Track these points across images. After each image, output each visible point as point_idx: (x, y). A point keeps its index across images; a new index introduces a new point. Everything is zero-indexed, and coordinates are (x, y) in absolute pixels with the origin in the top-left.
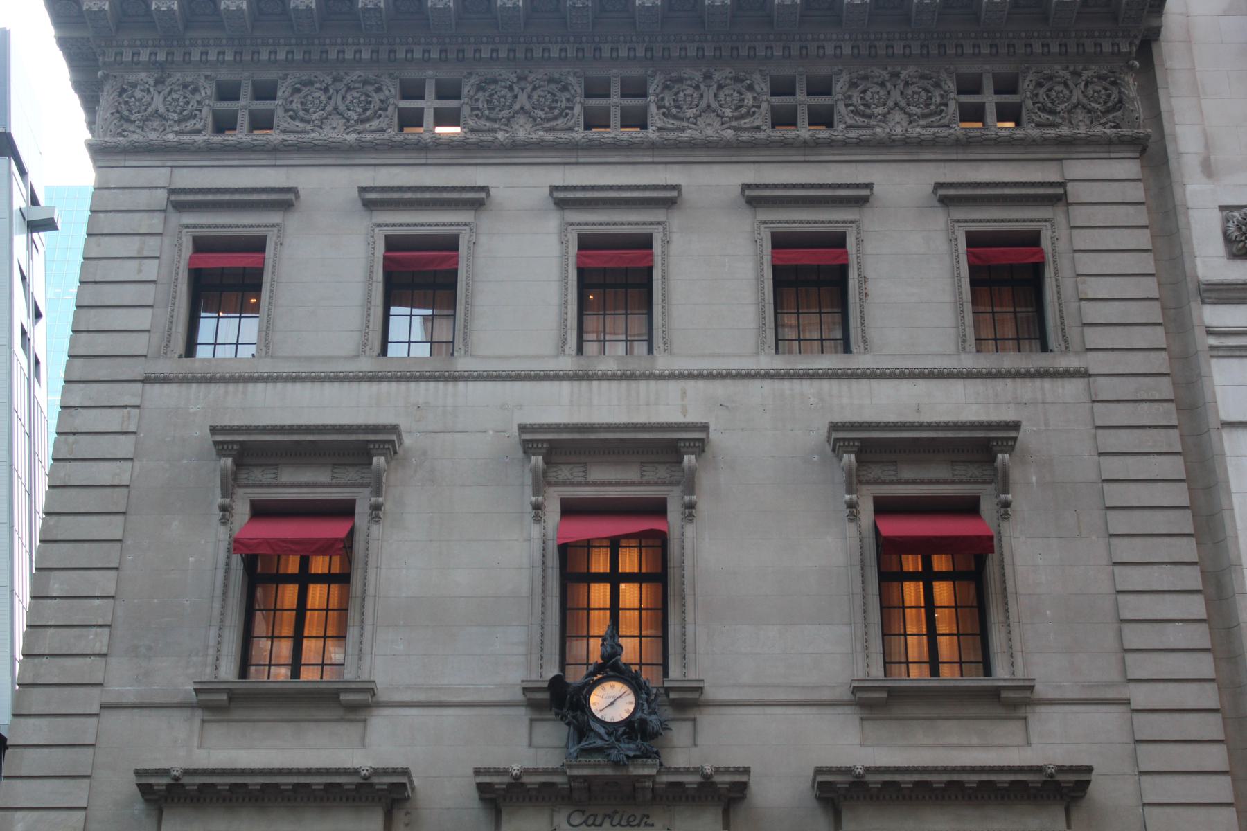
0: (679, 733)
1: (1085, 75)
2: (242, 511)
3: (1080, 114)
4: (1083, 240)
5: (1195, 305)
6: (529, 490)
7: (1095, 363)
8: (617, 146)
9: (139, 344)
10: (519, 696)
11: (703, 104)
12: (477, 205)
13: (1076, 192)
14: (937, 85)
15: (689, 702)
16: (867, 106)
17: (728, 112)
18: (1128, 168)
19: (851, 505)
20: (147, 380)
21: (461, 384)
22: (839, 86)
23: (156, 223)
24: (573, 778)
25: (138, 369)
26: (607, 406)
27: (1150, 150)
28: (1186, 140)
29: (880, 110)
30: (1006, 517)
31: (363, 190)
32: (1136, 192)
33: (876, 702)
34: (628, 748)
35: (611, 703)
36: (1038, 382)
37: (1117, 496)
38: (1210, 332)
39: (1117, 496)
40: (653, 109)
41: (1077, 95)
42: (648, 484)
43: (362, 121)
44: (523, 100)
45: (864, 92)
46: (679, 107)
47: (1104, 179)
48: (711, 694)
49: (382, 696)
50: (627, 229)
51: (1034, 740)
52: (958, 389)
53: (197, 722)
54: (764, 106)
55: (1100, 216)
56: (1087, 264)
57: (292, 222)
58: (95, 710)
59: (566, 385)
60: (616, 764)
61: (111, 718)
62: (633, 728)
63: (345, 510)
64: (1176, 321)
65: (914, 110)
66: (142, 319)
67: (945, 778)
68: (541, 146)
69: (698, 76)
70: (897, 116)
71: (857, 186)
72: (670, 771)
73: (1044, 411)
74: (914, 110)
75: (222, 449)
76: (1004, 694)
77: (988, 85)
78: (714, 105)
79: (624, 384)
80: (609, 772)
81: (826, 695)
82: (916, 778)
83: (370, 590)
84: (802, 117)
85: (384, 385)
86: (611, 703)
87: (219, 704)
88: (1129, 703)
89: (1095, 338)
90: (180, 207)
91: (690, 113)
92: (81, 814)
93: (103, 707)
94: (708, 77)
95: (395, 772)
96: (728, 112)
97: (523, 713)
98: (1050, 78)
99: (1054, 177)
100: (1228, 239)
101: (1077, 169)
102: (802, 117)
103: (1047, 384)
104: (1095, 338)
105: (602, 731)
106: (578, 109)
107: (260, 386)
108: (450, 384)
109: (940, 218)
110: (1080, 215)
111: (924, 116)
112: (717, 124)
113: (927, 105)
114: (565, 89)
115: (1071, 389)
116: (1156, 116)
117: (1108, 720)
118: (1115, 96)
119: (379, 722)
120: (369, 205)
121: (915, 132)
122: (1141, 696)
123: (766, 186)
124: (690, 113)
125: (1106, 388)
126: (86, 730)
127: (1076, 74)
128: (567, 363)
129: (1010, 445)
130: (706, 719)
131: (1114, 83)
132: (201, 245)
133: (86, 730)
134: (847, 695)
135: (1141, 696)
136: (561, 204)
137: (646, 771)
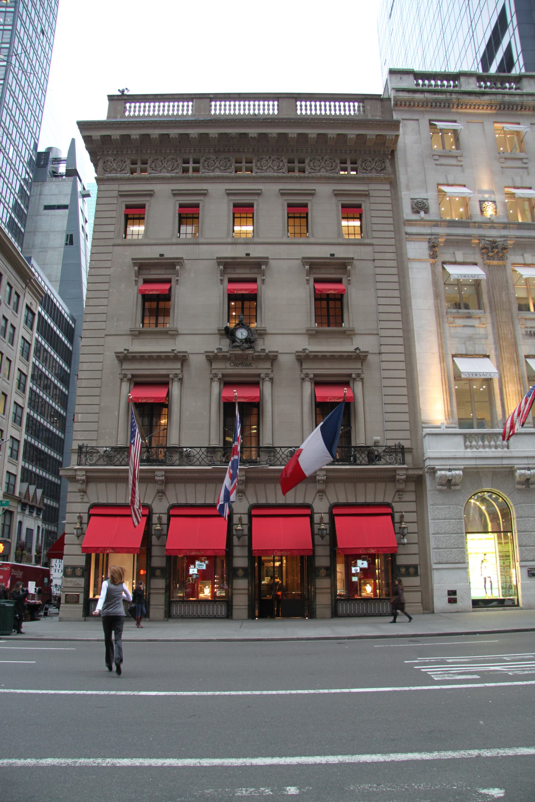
1: (376, 159)
2: (141, 282)
3: (374, 171)
4: (373, 207)
6: (219, 275)
7: (374, 241)
8: (244, 178)
9: (111, 235)
10: (217, 332)
11: (268, 165)
12: (205, 195)
13: (372, 193)
14: (334, 161)
15: (262, 333)
16: (315, 167)
17: (276, 168)
18: (387, 187)
19: (307, 280)
20: (113, 245)
21: (200, 246)
22: (307, 161)
23: (115, 201)
24: (231, 354)
25: (111, 242)
28: (402, 179)
29: (318, 168)
30: (349, 284)
31: (172, 190)
32: (388, 194)
34: (246, 345)
35: (242, 334)
36: (359, 247)
37: (379, 278)
38: (406, 234)
39: (379, 278)
41: (373, 165)
42: (252, 274)
43: (172, 170)
45: (314, 163)
46: (262, 166)
47: (379, 191)
48: (268, 331)
49: (180, 332)
51: (354, 344)
53: (131, 339)
54: (286, 166)
55: (378, 200)
56: (374, 213)
58: (104, 336)
59: (230, 247)
60: (243, 350)
61: (108, 338)
62: (247, 340)
63: (169, 281)
64: (397, 230)
65: (328, 168)
66: (112, 228)
67: (330, 354)
69: (267, 157)
70: (323, 170)
71: (311, 190)
72: (257, 352)
74: (328, 168)
75: (135, 264)
76: (347, 332)
77: (349, 161)
78: (272, 166)
79: (245, 246)
80: (240, 352)
81: (299, 332)
83: (176, 303)
84: (297, 170)
85: (179, 246)
86: (242, 334)
87: (137, 334)
88: (378, 334)
89: (375, 234)
90: (121, 196)
91: (264, 168)
92: (101, 363)
93: (106, 335)
94: (270, 158)
95: (183, 352)
97: (218, 336)
98: (366, 160)
99: (366, 189)
100: (413, 208)
101: (372, 187)
102: (297, 170)
103: (362, 247)
104: (375, 234)
105: (239, 341)
106: (233, 167)
107: (145, 247)
108: (197, 246)
109: (334, 200)
110: (372, 200)
111: (331, 170)
112: (272, 171)
113: (331, 167)
114: (229, 161)
116: (394, 171)
117: (373, 339)
118: (383, 166)
119: (179, 339)
120: (174, 195)
122: (383, 333)
124: (264, 168)
125: (377, 249)
126: (101, 342)
127: (373, 159)
129: (351, 264)
130: (268, 339)
131: (383, 162)
132: (128, 207)
133: (101, 342)
135: (383, 333)
137: (250, 352)
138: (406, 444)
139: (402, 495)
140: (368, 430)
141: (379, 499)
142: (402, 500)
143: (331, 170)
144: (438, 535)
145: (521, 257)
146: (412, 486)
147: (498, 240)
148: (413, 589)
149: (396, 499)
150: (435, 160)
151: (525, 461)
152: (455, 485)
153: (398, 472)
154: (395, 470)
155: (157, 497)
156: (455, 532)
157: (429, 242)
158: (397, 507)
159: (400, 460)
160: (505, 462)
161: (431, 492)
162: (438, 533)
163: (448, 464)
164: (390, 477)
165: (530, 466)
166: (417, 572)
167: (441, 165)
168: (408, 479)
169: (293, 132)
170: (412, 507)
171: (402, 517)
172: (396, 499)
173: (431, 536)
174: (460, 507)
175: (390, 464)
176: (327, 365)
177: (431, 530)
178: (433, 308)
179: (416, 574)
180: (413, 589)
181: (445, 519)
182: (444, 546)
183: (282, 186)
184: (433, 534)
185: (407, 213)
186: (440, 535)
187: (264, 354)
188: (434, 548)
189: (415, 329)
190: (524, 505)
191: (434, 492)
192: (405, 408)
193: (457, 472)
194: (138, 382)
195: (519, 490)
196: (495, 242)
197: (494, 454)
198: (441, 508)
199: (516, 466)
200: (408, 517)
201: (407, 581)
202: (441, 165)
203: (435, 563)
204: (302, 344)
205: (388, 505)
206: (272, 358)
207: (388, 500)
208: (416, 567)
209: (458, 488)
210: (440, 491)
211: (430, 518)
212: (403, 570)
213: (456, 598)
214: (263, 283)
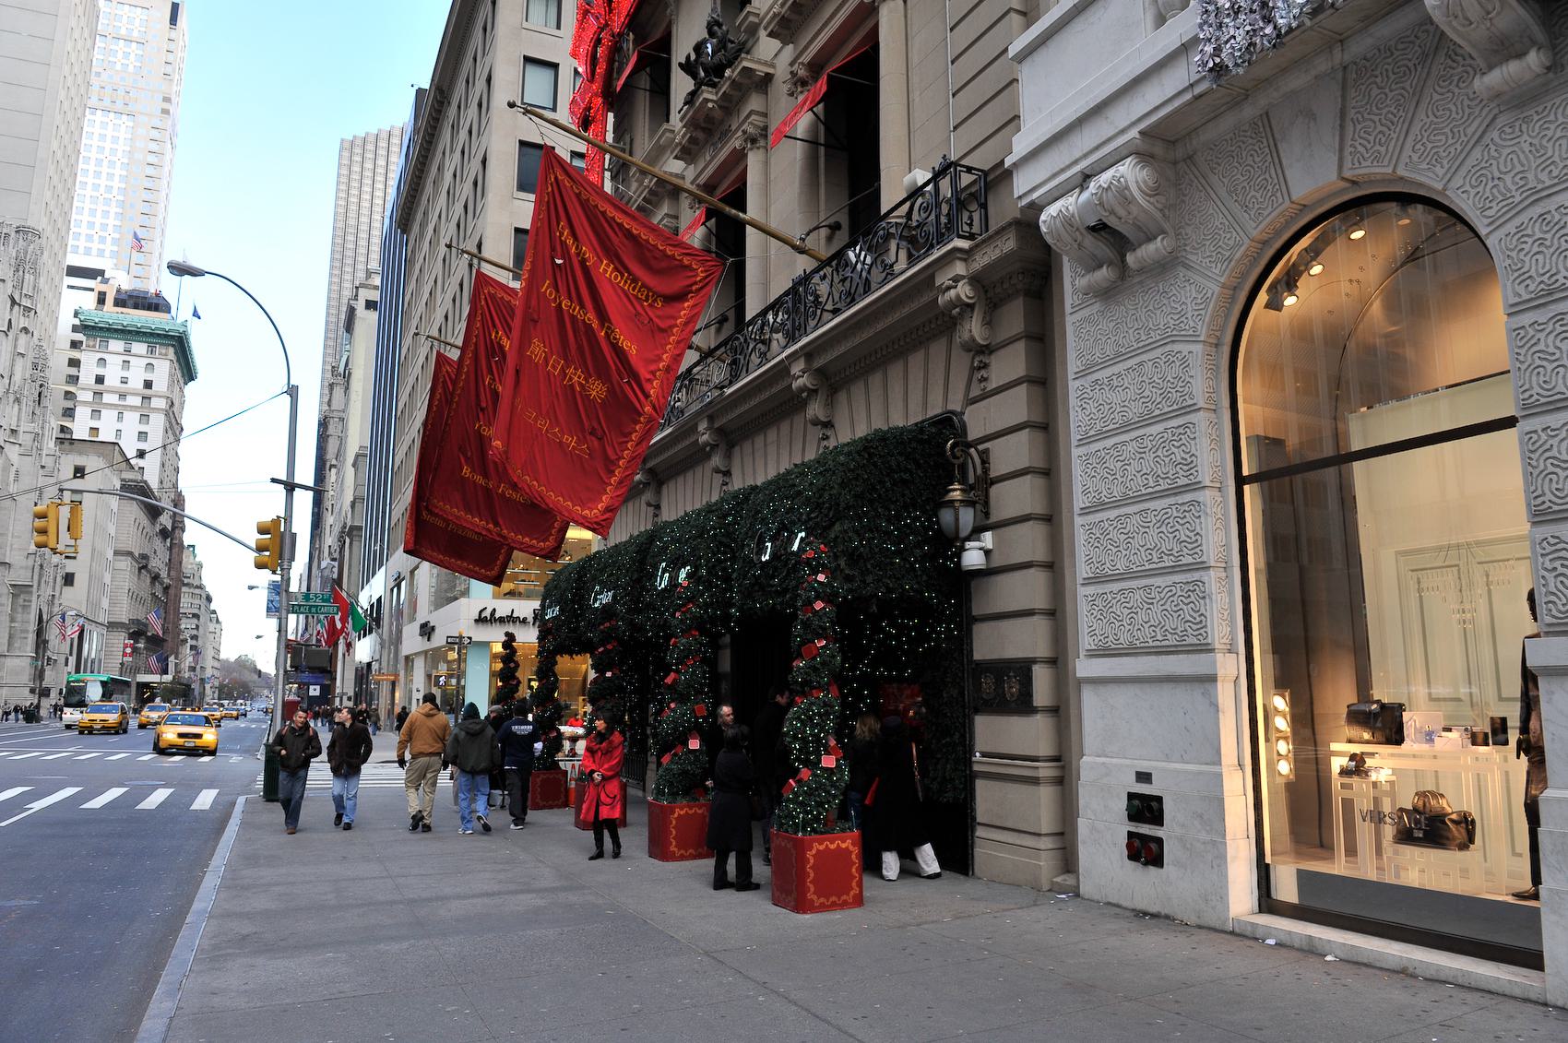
139: (985, 366)
142: (993, 385)
144: (1099, 516)
148: (1016, 771)
158: (978, 422)
163: (1078, 154)
166: (1031, 696)
168: (991, 291)
170: (1015, 407)
171: (985, 458)
173: (1078, 521)
174: (1185, 348)
177: (1079, 501)
179: (1024, 705)
180: (1016, 771)
184: (1086, 512)
188: (1089, 582)
193: (1105, 178)
198: (1110, 379)
200: (1011, 454)
201: (992, 733)
203: (1093, 654)
208: (1022, 669)
211: (1075, 438)
212: (987, 683)
213: (1160, 841)
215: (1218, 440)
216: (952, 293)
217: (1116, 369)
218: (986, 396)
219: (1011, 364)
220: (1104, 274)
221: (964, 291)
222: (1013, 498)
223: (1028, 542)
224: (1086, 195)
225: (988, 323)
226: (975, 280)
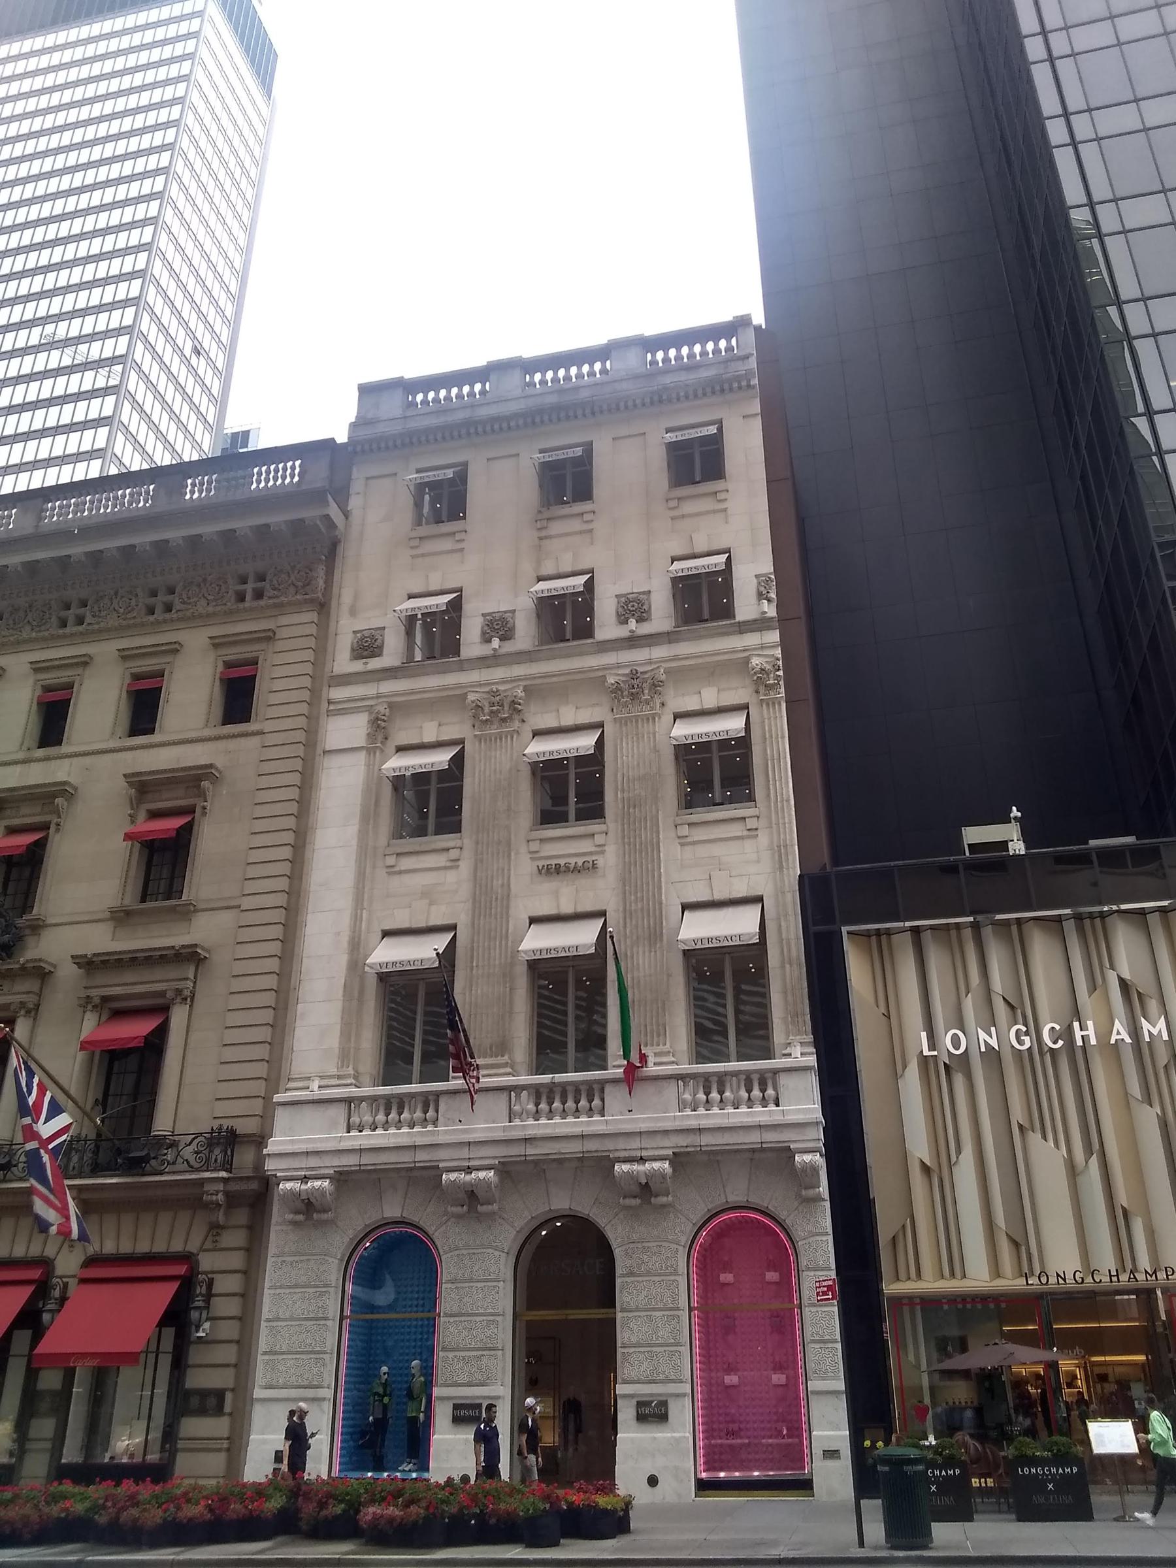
0: (30, 941)
4: (279, 659)
5: (325, 689)
7: (268, 726)
15: (37, 927)
18: (313, 616)
19: (130, 815)
26: (37, 774)
27: (323, 607)
28: (345, 596)
33: (121, 917)
40: (88, 614)
44: (29, 618)
48: (50, 921)
50: (149, 669)
52: (199, 748)
57: (88, 672)
59: (18, 768)
68: (35, 640)
73: (235, 755)
82: (130, 956)
96: (121, 611)
100: (353, 650)
101: (284, 620)
103: (243, 741)
110: (280, 645)
115: (254, 741)
121: (210, 609)
122: (246, 903)
123: (229, 635)
125: (271, 739)
128: (20, 756)
134: (108, 915)
135: (246, 903)
136: (37, 670)
138: (245, 1127)
140: (187, 1101)
141: (177, 1246)
143: (215, 600)
144: (275, 1324)
145: (554, 714)
146: (241, 1216)
147: (501, 688)
149: (209, 1245)
150: (412, 548)
151: (465, 1153)
152: (325, 1211)
153: (207, 1187)
154: (202, 1182)
155: (66, 1245)
156: (312, 1316)
157: (371, 713)
158: (207, 1262)
159: (216, 1160)
160: (422, 1156)
161: (279, 1228)
162: (278, 1319)
164: (189, 1199)
165: (471, 1163)
167: (423, 555)
168: (233, 1200)
169: (242, 524)
170: (236, 1260)
172: (209, 1245)
173: (263, 1324)
175: (198, 1170)
176: (129, 976)
178: (354, 842)
181: (296, 1286)
182: (284, 1349)
183: (124, 643)
184: (268, 1320)
185: (343, 662)
186: (280, 1323)
187: (17, 966)
189: (313, 888)
190: (465, 1252)
191: (284, 1228)
192: (262, 1052)
193: (317, 1183)
194: (117, 1010)
195: (459, 1217)
196: (495, 693)
197: (677, 1123)
199: (441, 1165)
200: (227, 1284)
202: (423, 555)
204: (102, 940)
205: (187, 1258)
206: (42, 974)
207: (193, 1247)
209: (325, 1216)
210: (295, 1223)
211: (267, 1285)
214: (58, 830)
215: (336, 1299)
216: (214, 1197)
217: (296, 1258)
218: (215, 1250)
219: (235, 1238)
220: (301, 1217)
221: (220, 1197)
222: (225, 1307)
223: (229, 1330)
224: (304, 1187)
225: (225, 1214)
226: (227, 1194)
